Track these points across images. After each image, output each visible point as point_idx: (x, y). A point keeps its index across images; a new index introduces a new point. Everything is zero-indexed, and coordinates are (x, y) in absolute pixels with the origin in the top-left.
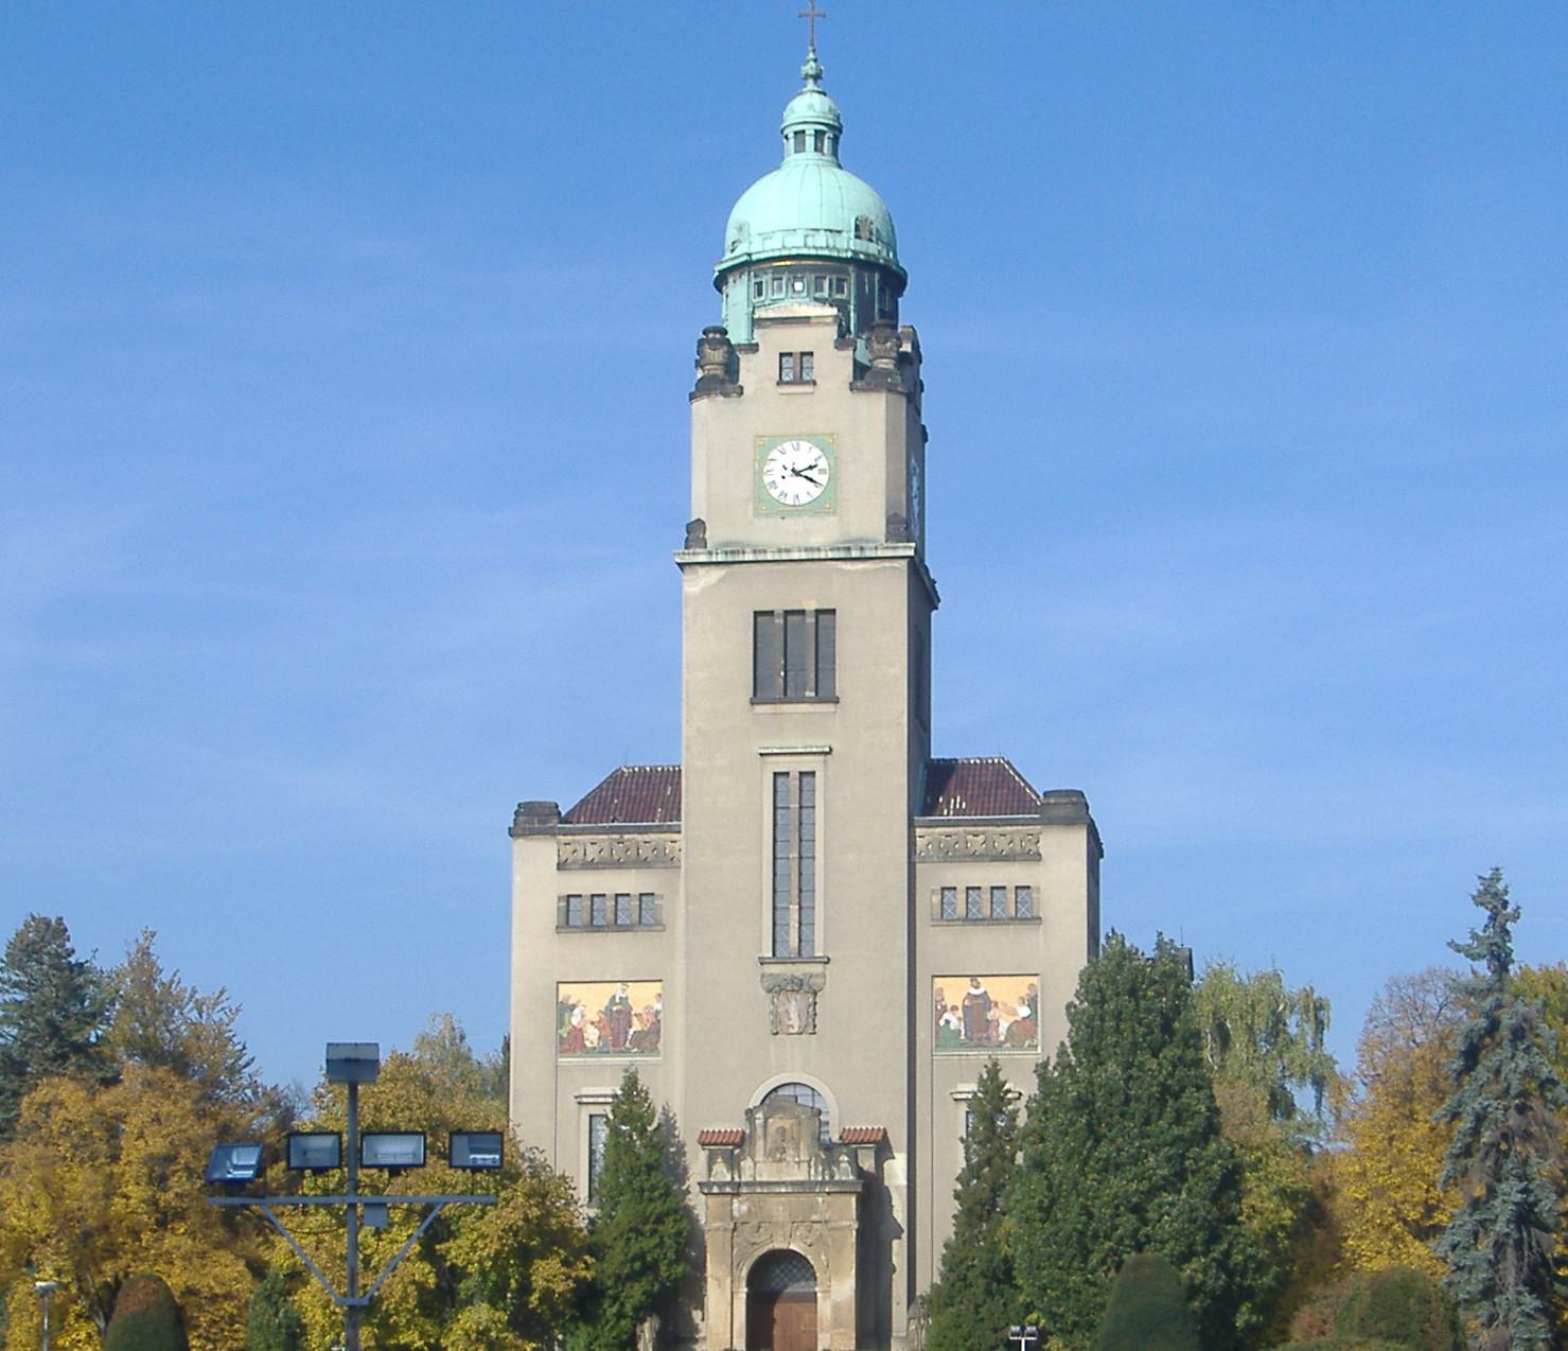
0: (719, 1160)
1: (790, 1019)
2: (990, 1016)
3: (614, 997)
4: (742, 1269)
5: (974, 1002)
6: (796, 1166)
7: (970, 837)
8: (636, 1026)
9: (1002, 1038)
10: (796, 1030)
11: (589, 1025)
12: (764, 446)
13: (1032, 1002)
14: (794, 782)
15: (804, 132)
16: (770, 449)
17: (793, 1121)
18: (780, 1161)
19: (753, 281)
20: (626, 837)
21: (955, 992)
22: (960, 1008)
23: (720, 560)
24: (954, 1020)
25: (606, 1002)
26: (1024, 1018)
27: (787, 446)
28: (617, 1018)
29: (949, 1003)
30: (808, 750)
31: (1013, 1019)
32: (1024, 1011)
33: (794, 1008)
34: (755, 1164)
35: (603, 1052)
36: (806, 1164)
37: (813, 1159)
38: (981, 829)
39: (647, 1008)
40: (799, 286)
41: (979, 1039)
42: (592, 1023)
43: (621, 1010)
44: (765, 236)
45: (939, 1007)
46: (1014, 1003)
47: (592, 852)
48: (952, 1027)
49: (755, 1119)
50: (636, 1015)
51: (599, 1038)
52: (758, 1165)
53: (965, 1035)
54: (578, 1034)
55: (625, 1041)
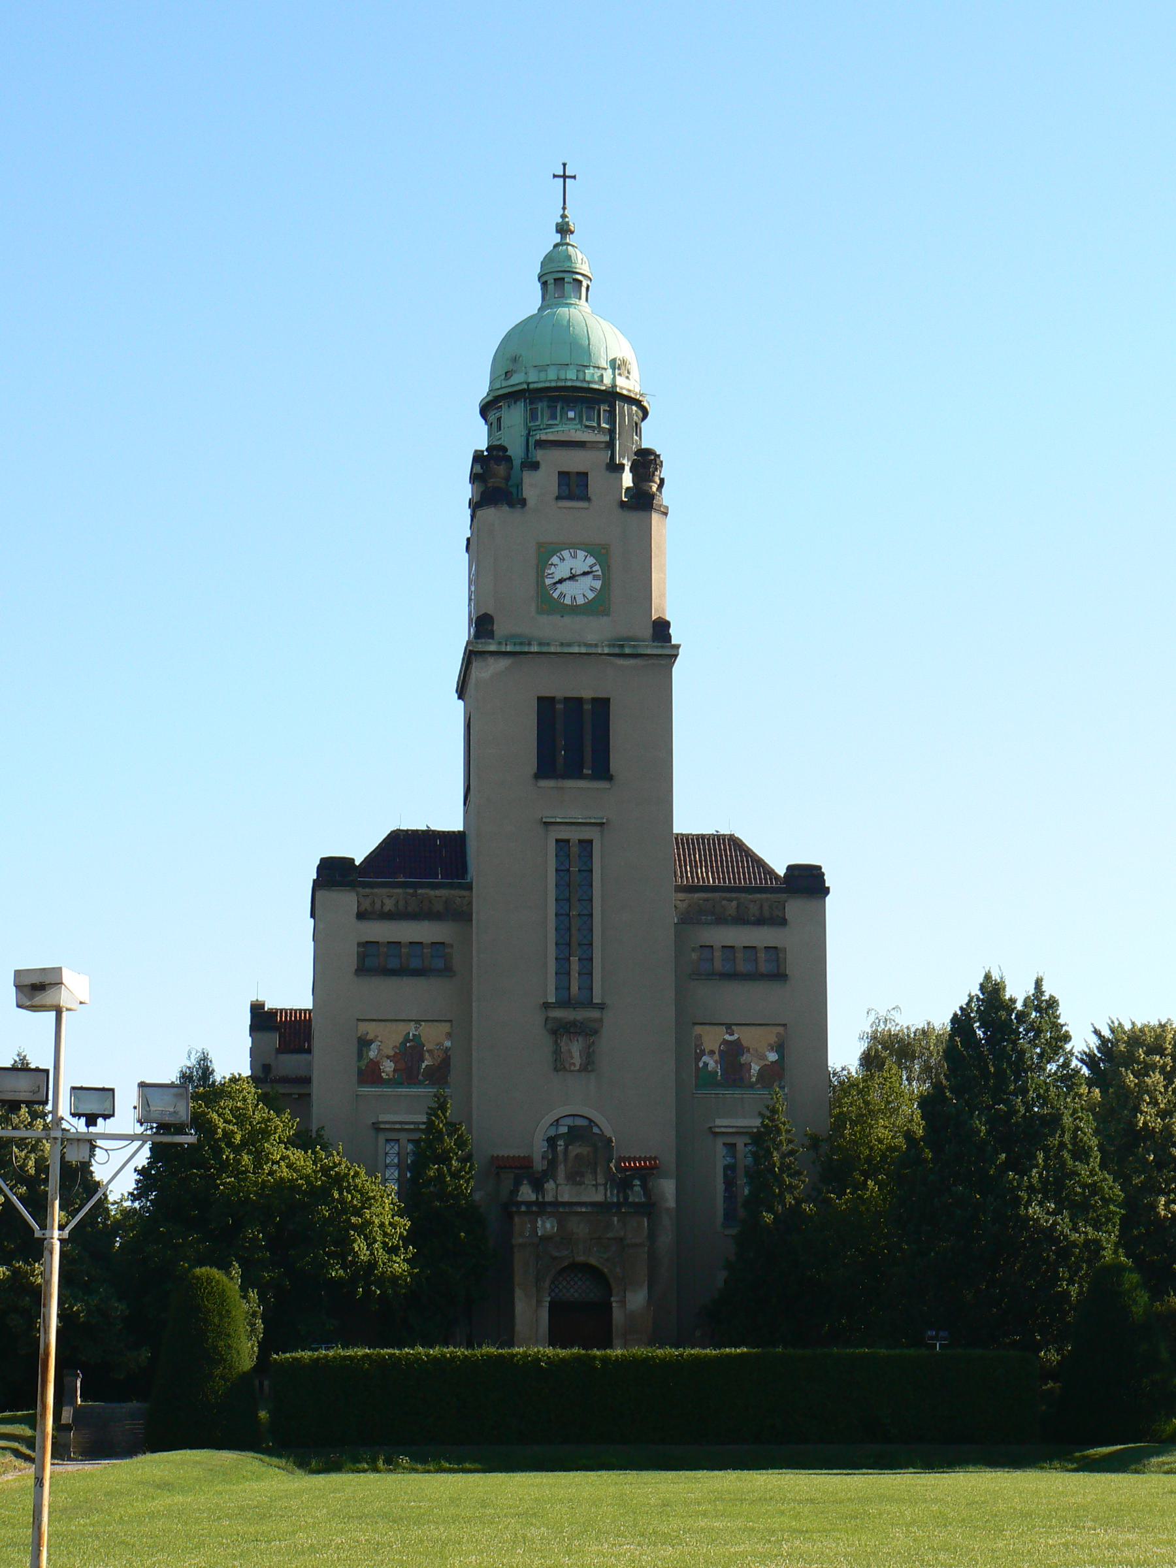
1: (572, 1058)
2: (743, 1059)
3: (409, 1033)
7: (724, 902)
9: (754, 1079)
12: (545, 553)
13: (780, 1048)
14: (575, 850)
15: (564, 279)
16: (553, 553)
18: (581, 1184)
19: (529, 408)
20: (419, 891)
21: (713, 1039)
23: (508, 650)
24: (711, 1062)
25: (401, 1040)
26: (772, 1062)
27: (566, 553)
28: (409, 1054)
29: (707, 1046)
30: (588, 821)
31: (763, 1063)
32: (773, 1057)
33: (575, 1049)
35: (400, 1084)
36: (601, 1189)
38: (734, 895)
39: (437, 1045)
40: (571, 414)
42: (388, 1057)
44: (542, 368)
47: (389, 905)
48: (710, 1068)
49: (557, 1145)
50: (428, 1051)
52: (559, 1188)
54: (375, 1066)
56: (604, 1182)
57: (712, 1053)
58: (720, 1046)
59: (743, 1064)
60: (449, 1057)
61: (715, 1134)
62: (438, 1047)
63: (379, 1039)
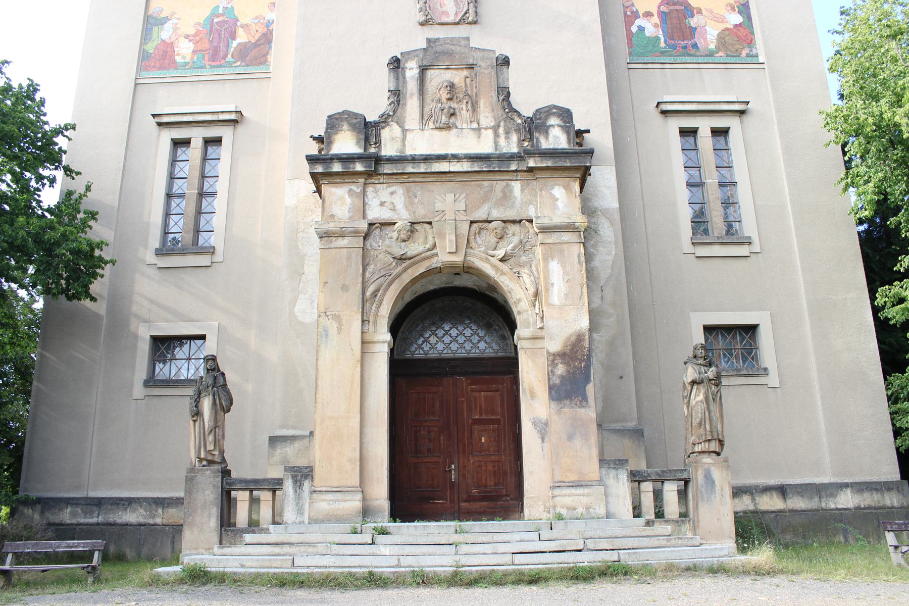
0: (345, 127)
2: (693, 22)
4: (381, 301)
5: (673, 8)
6: (472, 136)
8: (242, 37)
9: (712, 46)
10: (451, 19)
11: (182, 39)
17: (465, 73)
18: (447, 127)
22: (655, 13)
24: (651, 28)
25: (207, 13)
26: (736, 26)
31: (723, 26)
32: (736, 19)
34: (404, 131)
36: (490, 133)
37: (502, 124)
39: (257, 18)
41: (685, 47)
42: (187, 37)
43: (224, 21)
45: (629, 13)
46: (723, 11)
51: (194, 52)
52: (409, 136)
53: (665, 42)
55: (226, 56)
56: (492, 124)
57: (648, 14)
58: (659, 7)
59: (696, 28)
60: (271, 32)
61: (664, 112)
62: (257, 21)
63: (176, 16)
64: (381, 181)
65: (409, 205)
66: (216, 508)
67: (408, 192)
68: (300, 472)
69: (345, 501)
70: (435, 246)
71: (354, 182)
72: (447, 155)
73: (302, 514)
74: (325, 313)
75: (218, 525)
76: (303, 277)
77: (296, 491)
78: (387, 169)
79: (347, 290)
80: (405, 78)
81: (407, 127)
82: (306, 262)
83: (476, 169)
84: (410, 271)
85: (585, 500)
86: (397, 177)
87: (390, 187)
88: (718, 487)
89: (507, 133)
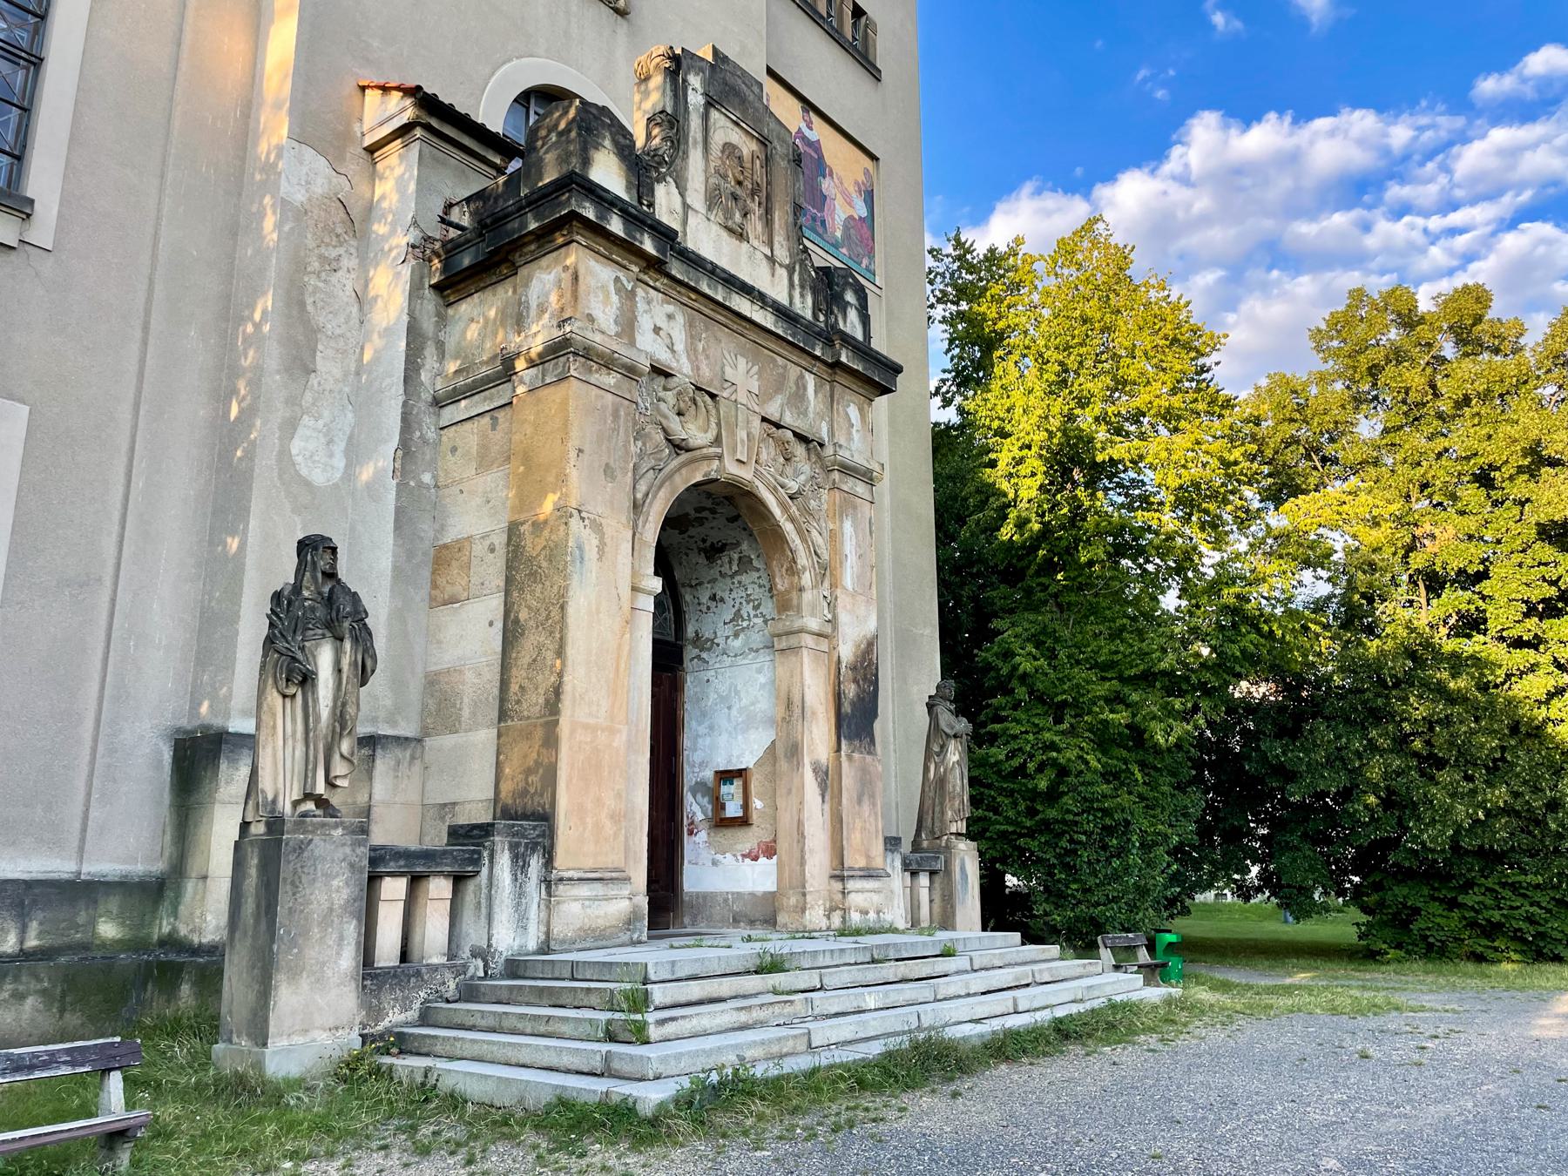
0: (607, 143)
9: (838, 234)
17: (754, 146)
31: (851, 212)
32: (862, 211)
36: (782, 273)
37: (797, 267)
41: (814, 219)
64: (658, 284)
65: (691, 351)
66: (354, 922)
67: (690, 326)
68: (524, 837)
69: (608, 899)
70: (717, 441)
71: (625, 267)
72: (753, 288)
73: (525, 928)
74: (580, 511)
75: (358, 966)
76: (314, 380)
77: (516, 880)
78: (676, 270)
79: (613, 478)
80: (686, 102)
81: (689, 201)
82: (320, 347)
83: (780, 332)
84: (684, 471)
85: (875, 898)
86: (683, 290)
87: (669, 303)
88: (970, 885)
89: (802, 287)
